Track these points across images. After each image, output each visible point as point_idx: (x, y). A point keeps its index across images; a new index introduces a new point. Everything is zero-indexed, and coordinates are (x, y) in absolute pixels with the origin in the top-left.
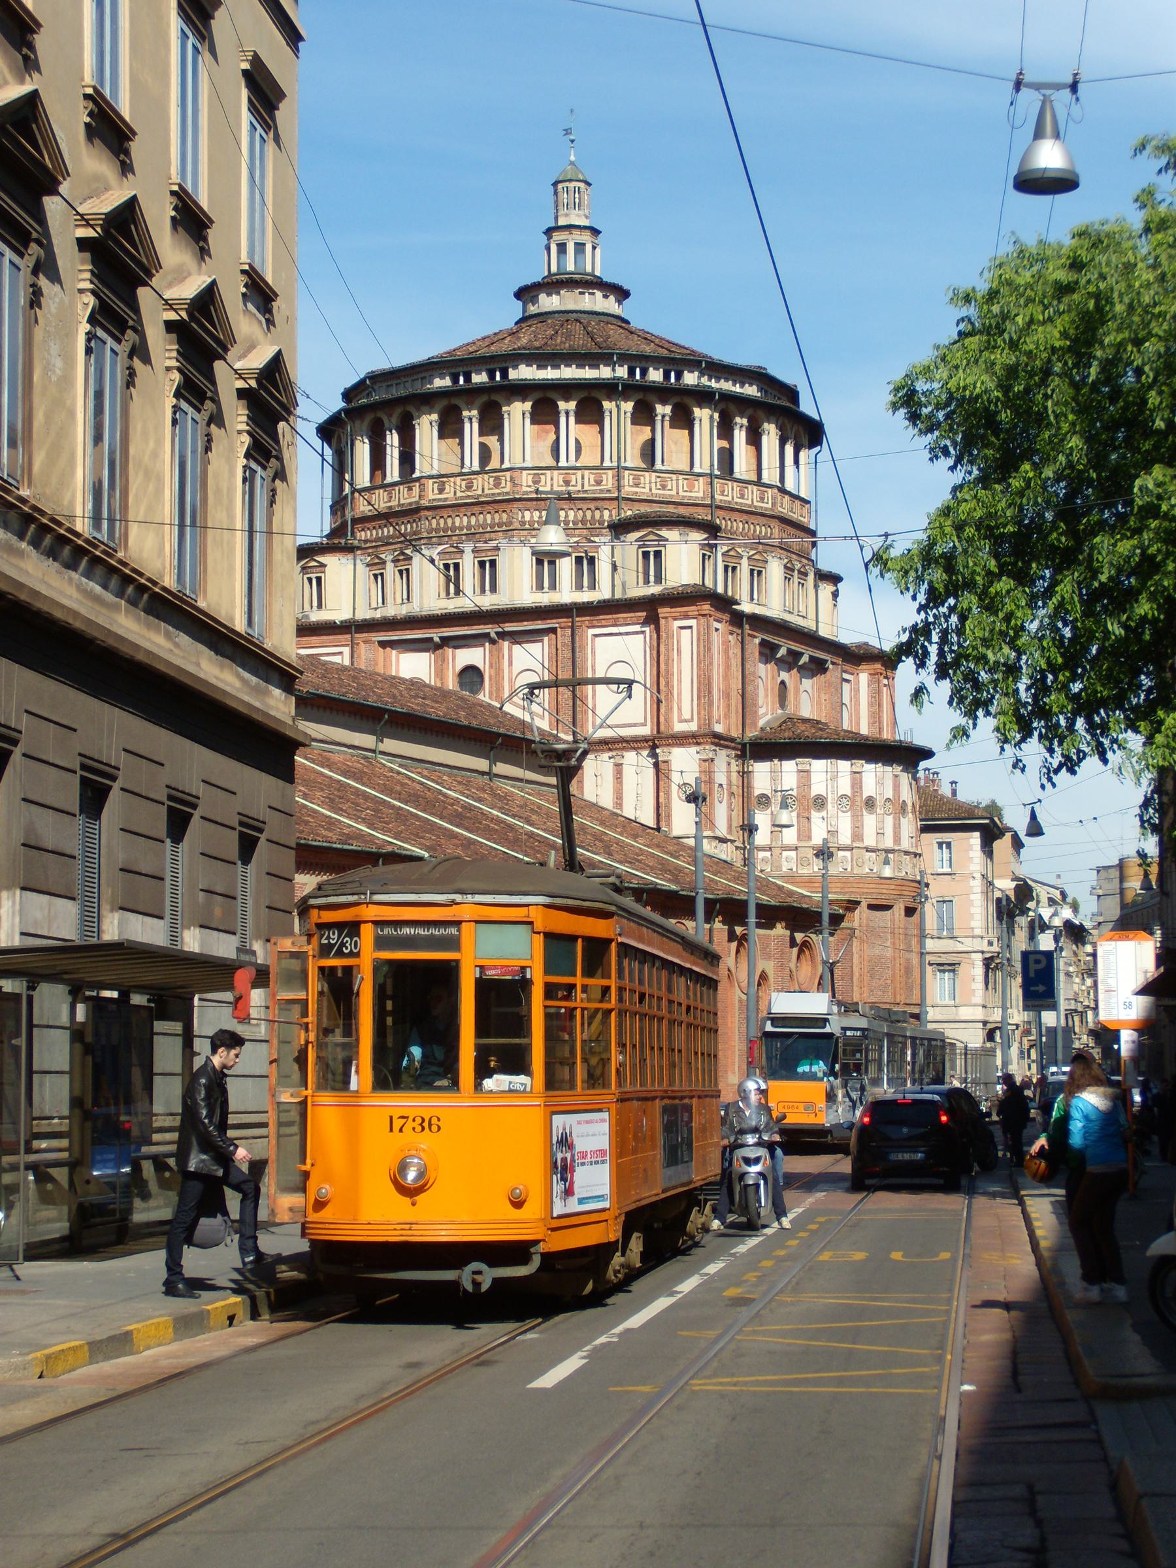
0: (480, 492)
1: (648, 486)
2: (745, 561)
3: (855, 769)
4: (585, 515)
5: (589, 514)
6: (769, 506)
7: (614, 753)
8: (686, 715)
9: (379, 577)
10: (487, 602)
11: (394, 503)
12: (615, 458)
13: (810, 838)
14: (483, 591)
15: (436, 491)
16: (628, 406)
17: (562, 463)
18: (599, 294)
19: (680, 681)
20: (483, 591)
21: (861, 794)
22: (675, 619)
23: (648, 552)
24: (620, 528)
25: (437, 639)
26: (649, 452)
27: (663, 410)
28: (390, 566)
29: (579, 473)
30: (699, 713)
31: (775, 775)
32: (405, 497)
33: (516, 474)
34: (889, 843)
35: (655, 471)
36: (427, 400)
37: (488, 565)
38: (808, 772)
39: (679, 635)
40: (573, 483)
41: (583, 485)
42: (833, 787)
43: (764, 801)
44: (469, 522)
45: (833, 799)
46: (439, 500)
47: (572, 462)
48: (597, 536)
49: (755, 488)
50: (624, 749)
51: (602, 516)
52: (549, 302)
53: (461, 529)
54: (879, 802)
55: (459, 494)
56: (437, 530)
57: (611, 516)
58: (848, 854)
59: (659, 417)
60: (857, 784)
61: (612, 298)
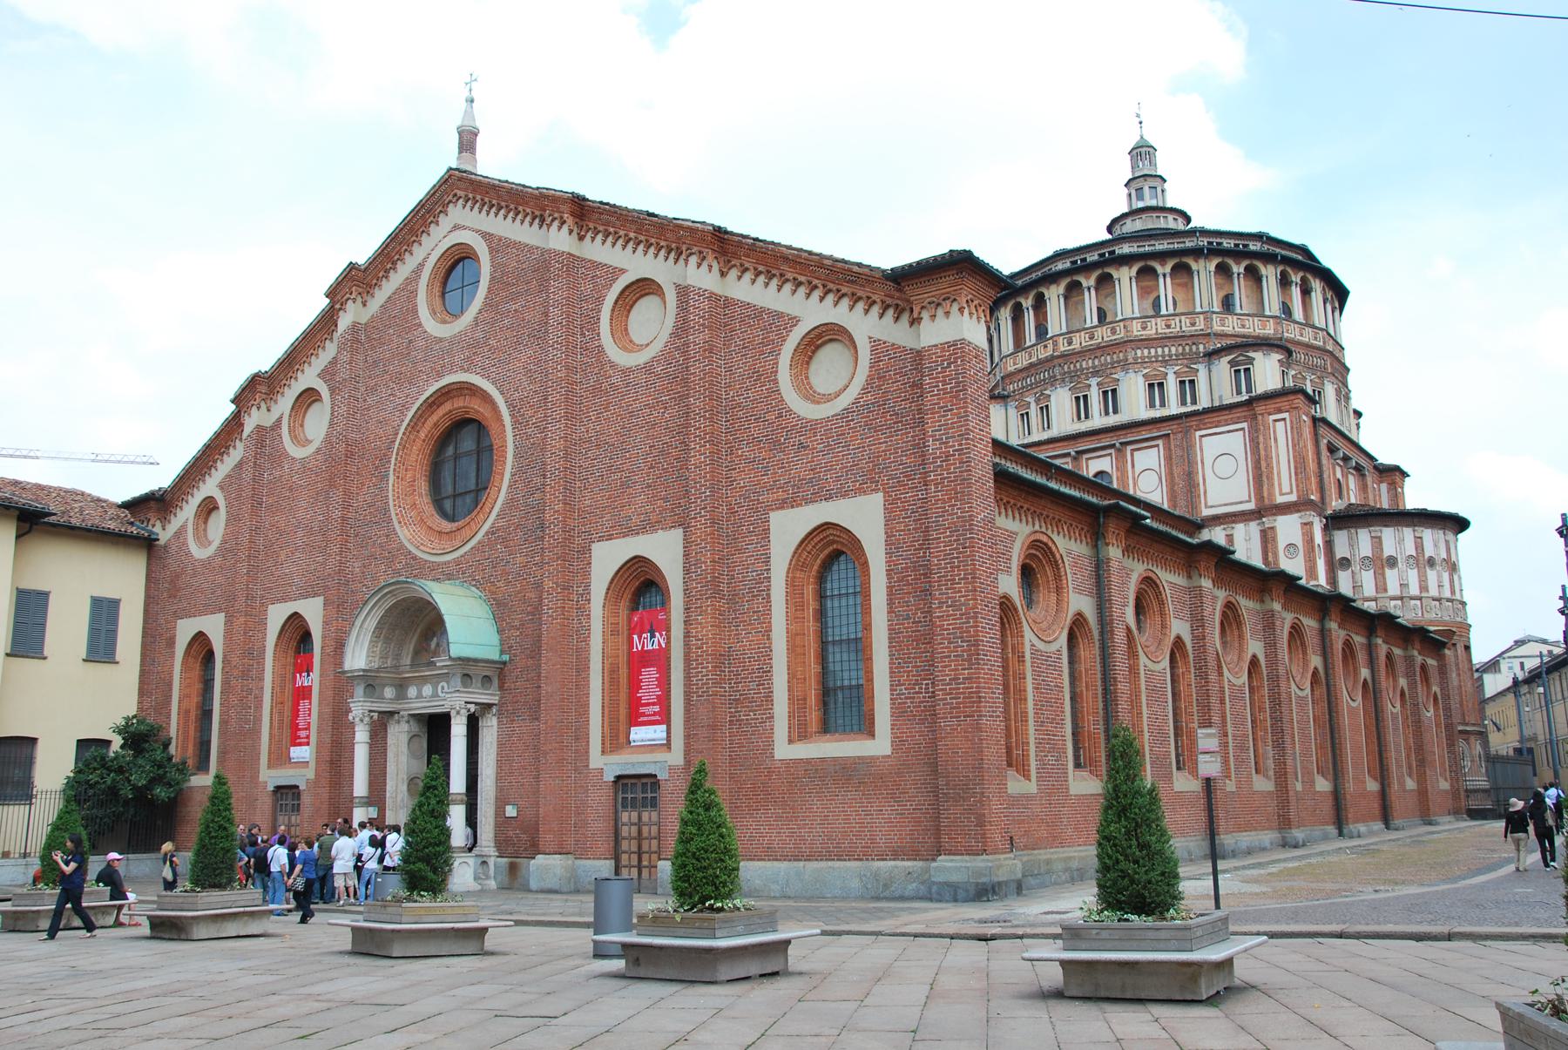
0: (1100, 340)
1: (1231, 325)
2: (1308, 383)
3: (1417, 535)
4: (1184, 349)
5: (1187, 348)
6: (1321, 344)
7: (1225, 526)
8: (1286, 489)
9: (1025, 416)
10: (1112, 420)
11: (1034, 359)
12: (1205, 304)
13: (1385, 590)
14: (1107, 413)
15: (1066, 344)
16: (1212, 265)
17: (1164, 311)
18: (1170, 217)
19: (1278, 462)
20: (1107, 413)
21: (1424, 556)
22: (1270, 414)
23: (1239, 370)
24: (1212, 355)
25: (1073, 453)
26: (1227, 304)
27: (1238, 268)
28: (1033, 405)
29: (1177, 319)
30: (1297, 486)
31: (1352, 544)
32: (1043, 354)
33: (1127, 323)
34: (1447, 594)
35: (1236, 315)
36: (1053, 278)
37: (1110, 393)
38: (1380, 538)
39: (1274, 427)
40: (1173, 326)
41: (1181, 328)
42: (1401, 549)
43: (1345, 563)
44: (1093, 363)
45: (1402, 559)
46: (1069, 350)
47: (1171, 310)
48: (1196, 364)
49: (1310, 329)
50: (1234, 522)
51: (1198, 349)
52: (1131, 226)
53: (1088, 369)
54: (1438, 561)
55: (1084, 344)
56: (1069, 372)
57: (1205, 348)
58: (1418, 602)
59: (1236, 275)
60: (1419, 545)
61: (1180, 220)
